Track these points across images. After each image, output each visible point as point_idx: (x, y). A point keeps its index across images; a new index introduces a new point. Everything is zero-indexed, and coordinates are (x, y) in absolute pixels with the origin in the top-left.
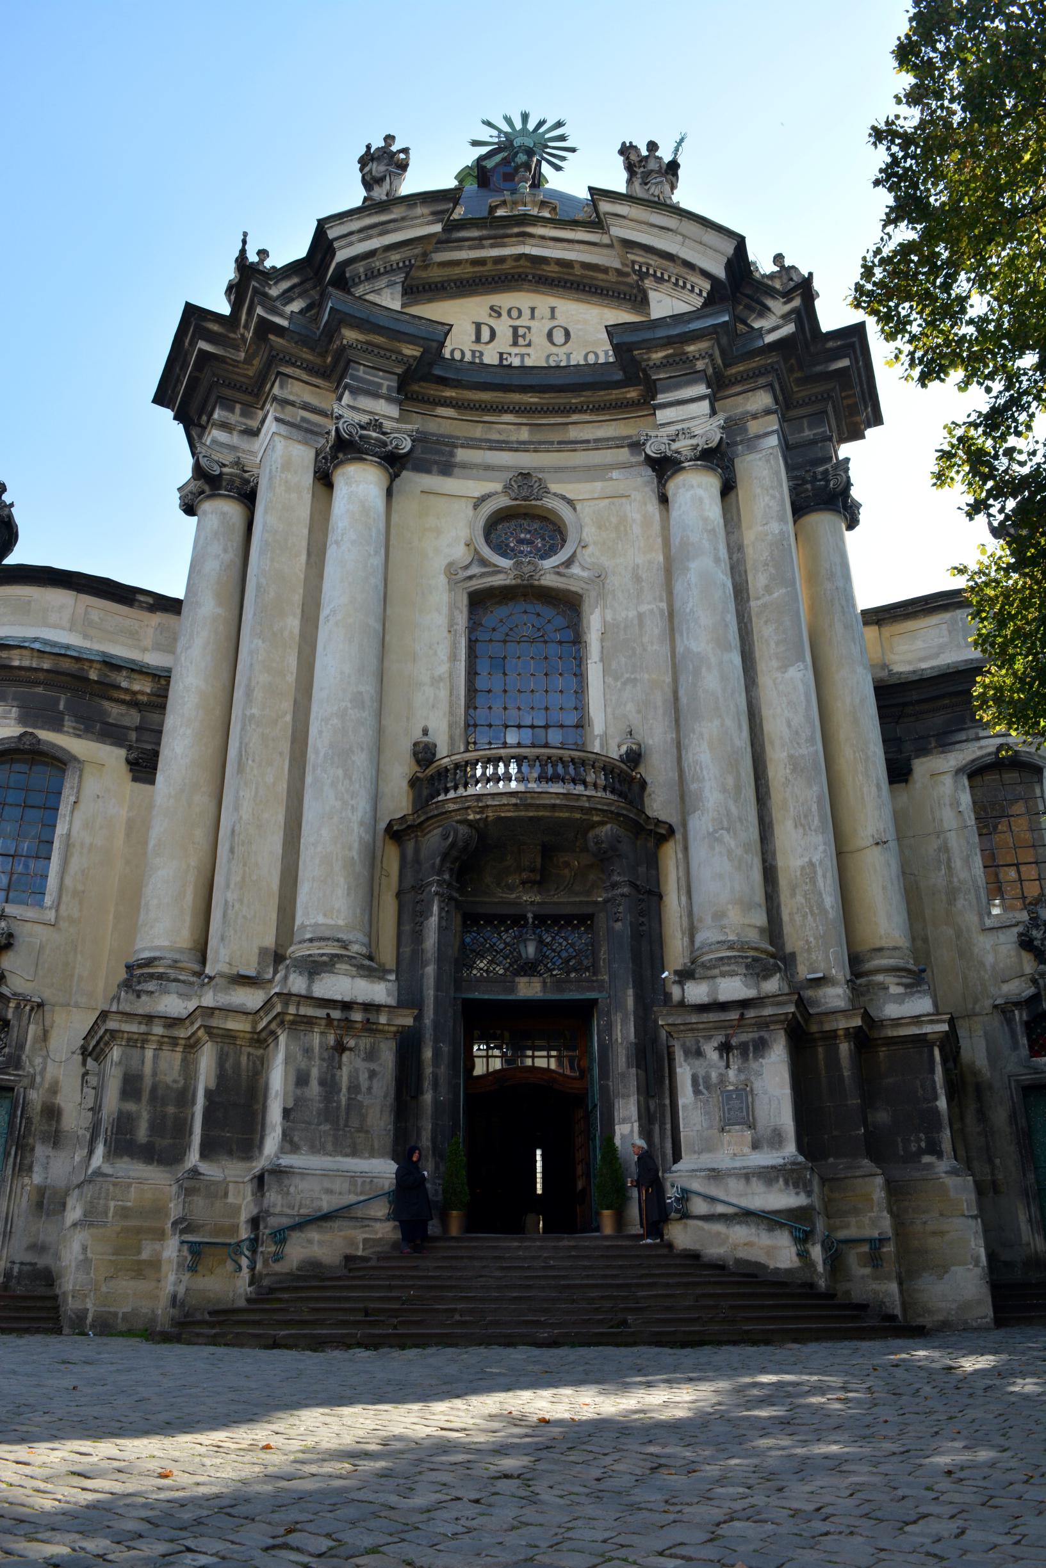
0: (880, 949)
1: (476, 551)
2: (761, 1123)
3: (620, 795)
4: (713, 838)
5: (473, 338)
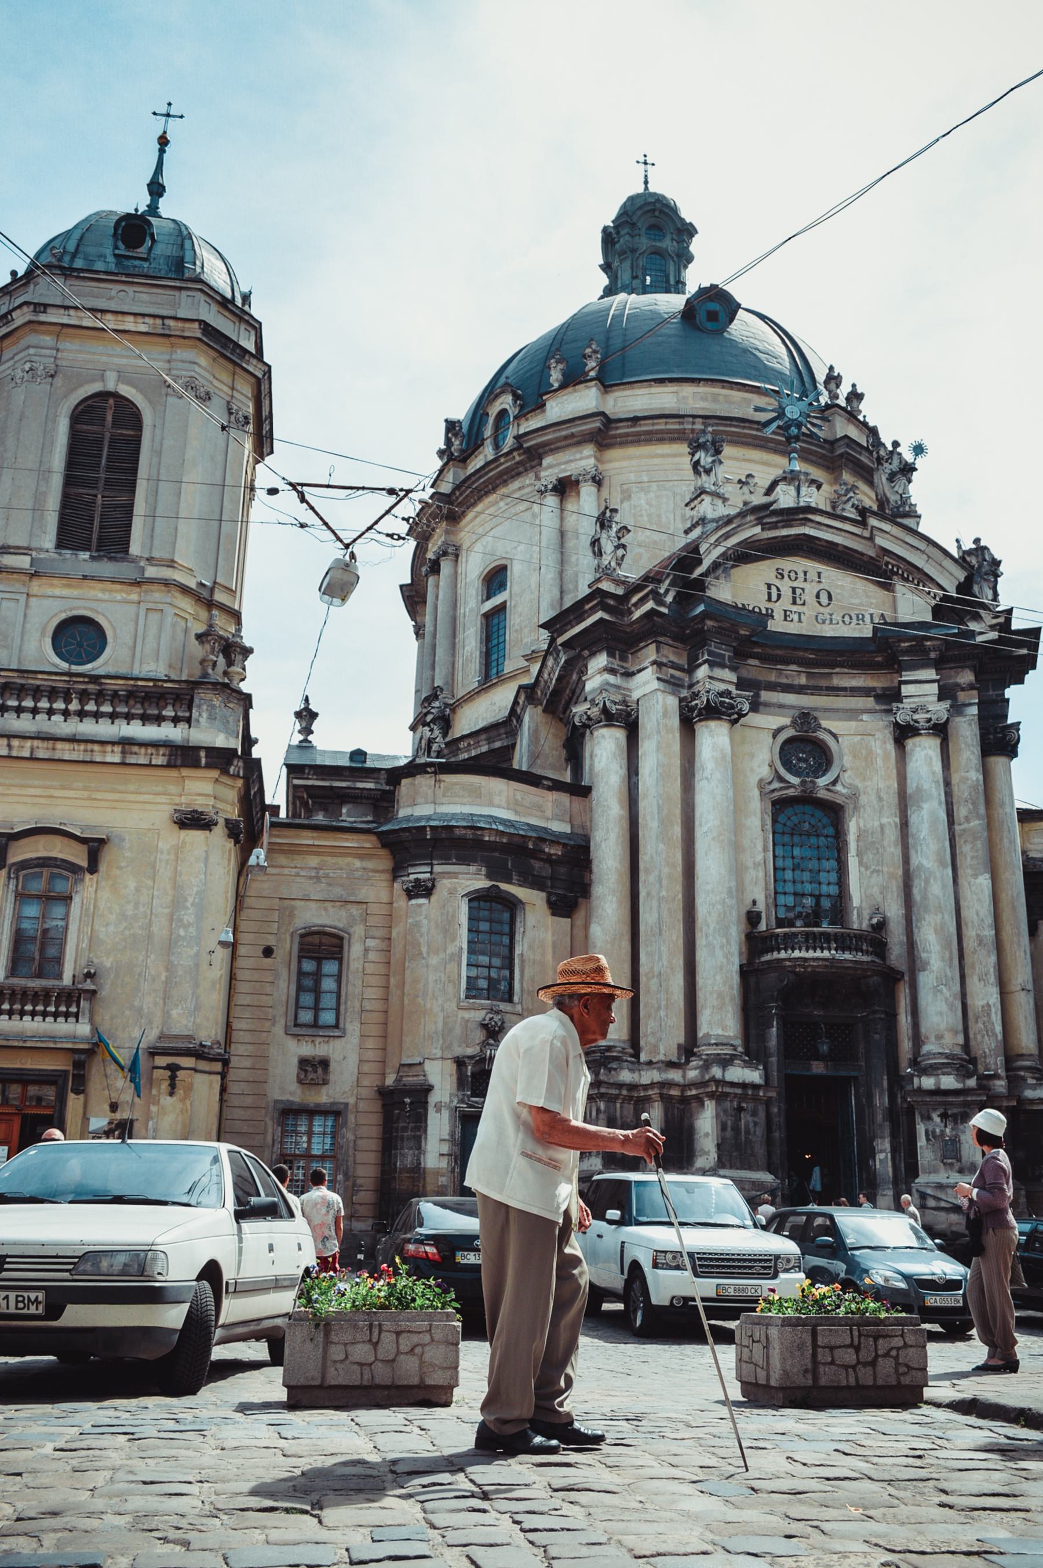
0: (1022, 1055)
1: (776, 771)
2: (965, 1158)
3: (877, 955)
4: (936, 990)
5: (766, 597)
